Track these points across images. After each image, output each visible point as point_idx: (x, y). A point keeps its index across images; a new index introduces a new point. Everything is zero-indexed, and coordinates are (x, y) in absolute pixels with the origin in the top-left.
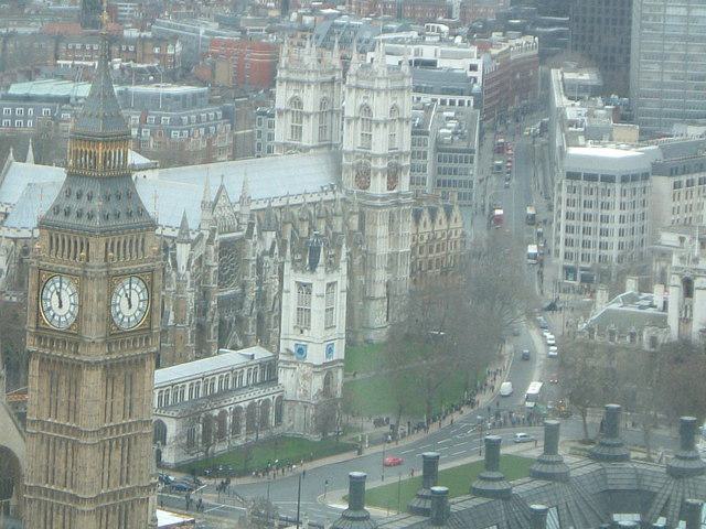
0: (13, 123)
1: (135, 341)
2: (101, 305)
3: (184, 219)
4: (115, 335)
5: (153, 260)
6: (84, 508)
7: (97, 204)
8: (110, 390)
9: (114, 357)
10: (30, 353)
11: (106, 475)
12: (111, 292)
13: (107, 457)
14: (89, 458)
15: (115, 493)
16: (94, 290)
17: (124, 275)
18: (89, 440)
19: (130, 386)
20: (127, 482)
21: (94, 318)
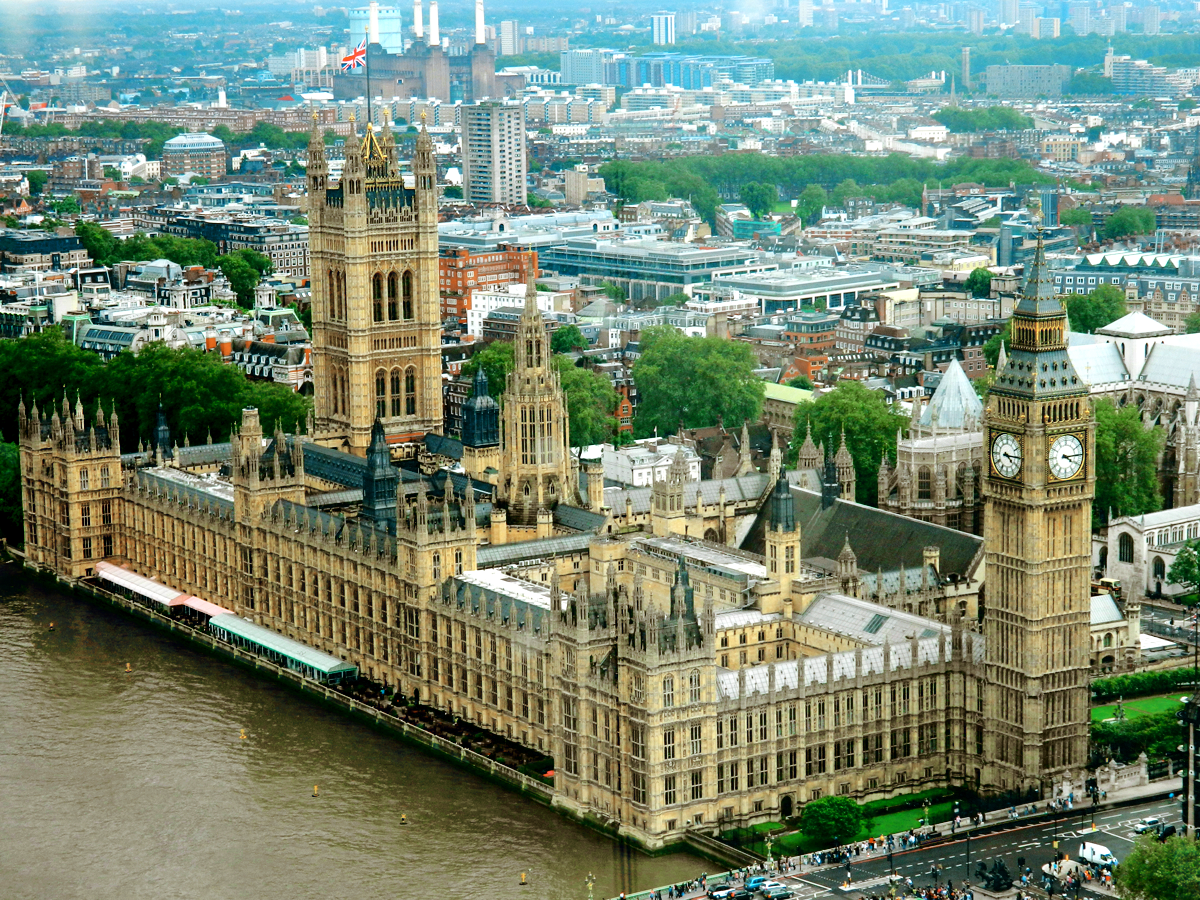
0: (1075, 290)
2: (1040, 458)
3: (1192, 380)
4: (1052, 485)
6: (1035, 629)
9: (1053, 501)
10: (985, 498)
11: (1051, 602)
12: (1048, 447)
13: (1051, 587)
14: (1037, 589)
15: (1059, 617)
17: (1059, 433)
19: (1069, 528)
21: (1034, 468)
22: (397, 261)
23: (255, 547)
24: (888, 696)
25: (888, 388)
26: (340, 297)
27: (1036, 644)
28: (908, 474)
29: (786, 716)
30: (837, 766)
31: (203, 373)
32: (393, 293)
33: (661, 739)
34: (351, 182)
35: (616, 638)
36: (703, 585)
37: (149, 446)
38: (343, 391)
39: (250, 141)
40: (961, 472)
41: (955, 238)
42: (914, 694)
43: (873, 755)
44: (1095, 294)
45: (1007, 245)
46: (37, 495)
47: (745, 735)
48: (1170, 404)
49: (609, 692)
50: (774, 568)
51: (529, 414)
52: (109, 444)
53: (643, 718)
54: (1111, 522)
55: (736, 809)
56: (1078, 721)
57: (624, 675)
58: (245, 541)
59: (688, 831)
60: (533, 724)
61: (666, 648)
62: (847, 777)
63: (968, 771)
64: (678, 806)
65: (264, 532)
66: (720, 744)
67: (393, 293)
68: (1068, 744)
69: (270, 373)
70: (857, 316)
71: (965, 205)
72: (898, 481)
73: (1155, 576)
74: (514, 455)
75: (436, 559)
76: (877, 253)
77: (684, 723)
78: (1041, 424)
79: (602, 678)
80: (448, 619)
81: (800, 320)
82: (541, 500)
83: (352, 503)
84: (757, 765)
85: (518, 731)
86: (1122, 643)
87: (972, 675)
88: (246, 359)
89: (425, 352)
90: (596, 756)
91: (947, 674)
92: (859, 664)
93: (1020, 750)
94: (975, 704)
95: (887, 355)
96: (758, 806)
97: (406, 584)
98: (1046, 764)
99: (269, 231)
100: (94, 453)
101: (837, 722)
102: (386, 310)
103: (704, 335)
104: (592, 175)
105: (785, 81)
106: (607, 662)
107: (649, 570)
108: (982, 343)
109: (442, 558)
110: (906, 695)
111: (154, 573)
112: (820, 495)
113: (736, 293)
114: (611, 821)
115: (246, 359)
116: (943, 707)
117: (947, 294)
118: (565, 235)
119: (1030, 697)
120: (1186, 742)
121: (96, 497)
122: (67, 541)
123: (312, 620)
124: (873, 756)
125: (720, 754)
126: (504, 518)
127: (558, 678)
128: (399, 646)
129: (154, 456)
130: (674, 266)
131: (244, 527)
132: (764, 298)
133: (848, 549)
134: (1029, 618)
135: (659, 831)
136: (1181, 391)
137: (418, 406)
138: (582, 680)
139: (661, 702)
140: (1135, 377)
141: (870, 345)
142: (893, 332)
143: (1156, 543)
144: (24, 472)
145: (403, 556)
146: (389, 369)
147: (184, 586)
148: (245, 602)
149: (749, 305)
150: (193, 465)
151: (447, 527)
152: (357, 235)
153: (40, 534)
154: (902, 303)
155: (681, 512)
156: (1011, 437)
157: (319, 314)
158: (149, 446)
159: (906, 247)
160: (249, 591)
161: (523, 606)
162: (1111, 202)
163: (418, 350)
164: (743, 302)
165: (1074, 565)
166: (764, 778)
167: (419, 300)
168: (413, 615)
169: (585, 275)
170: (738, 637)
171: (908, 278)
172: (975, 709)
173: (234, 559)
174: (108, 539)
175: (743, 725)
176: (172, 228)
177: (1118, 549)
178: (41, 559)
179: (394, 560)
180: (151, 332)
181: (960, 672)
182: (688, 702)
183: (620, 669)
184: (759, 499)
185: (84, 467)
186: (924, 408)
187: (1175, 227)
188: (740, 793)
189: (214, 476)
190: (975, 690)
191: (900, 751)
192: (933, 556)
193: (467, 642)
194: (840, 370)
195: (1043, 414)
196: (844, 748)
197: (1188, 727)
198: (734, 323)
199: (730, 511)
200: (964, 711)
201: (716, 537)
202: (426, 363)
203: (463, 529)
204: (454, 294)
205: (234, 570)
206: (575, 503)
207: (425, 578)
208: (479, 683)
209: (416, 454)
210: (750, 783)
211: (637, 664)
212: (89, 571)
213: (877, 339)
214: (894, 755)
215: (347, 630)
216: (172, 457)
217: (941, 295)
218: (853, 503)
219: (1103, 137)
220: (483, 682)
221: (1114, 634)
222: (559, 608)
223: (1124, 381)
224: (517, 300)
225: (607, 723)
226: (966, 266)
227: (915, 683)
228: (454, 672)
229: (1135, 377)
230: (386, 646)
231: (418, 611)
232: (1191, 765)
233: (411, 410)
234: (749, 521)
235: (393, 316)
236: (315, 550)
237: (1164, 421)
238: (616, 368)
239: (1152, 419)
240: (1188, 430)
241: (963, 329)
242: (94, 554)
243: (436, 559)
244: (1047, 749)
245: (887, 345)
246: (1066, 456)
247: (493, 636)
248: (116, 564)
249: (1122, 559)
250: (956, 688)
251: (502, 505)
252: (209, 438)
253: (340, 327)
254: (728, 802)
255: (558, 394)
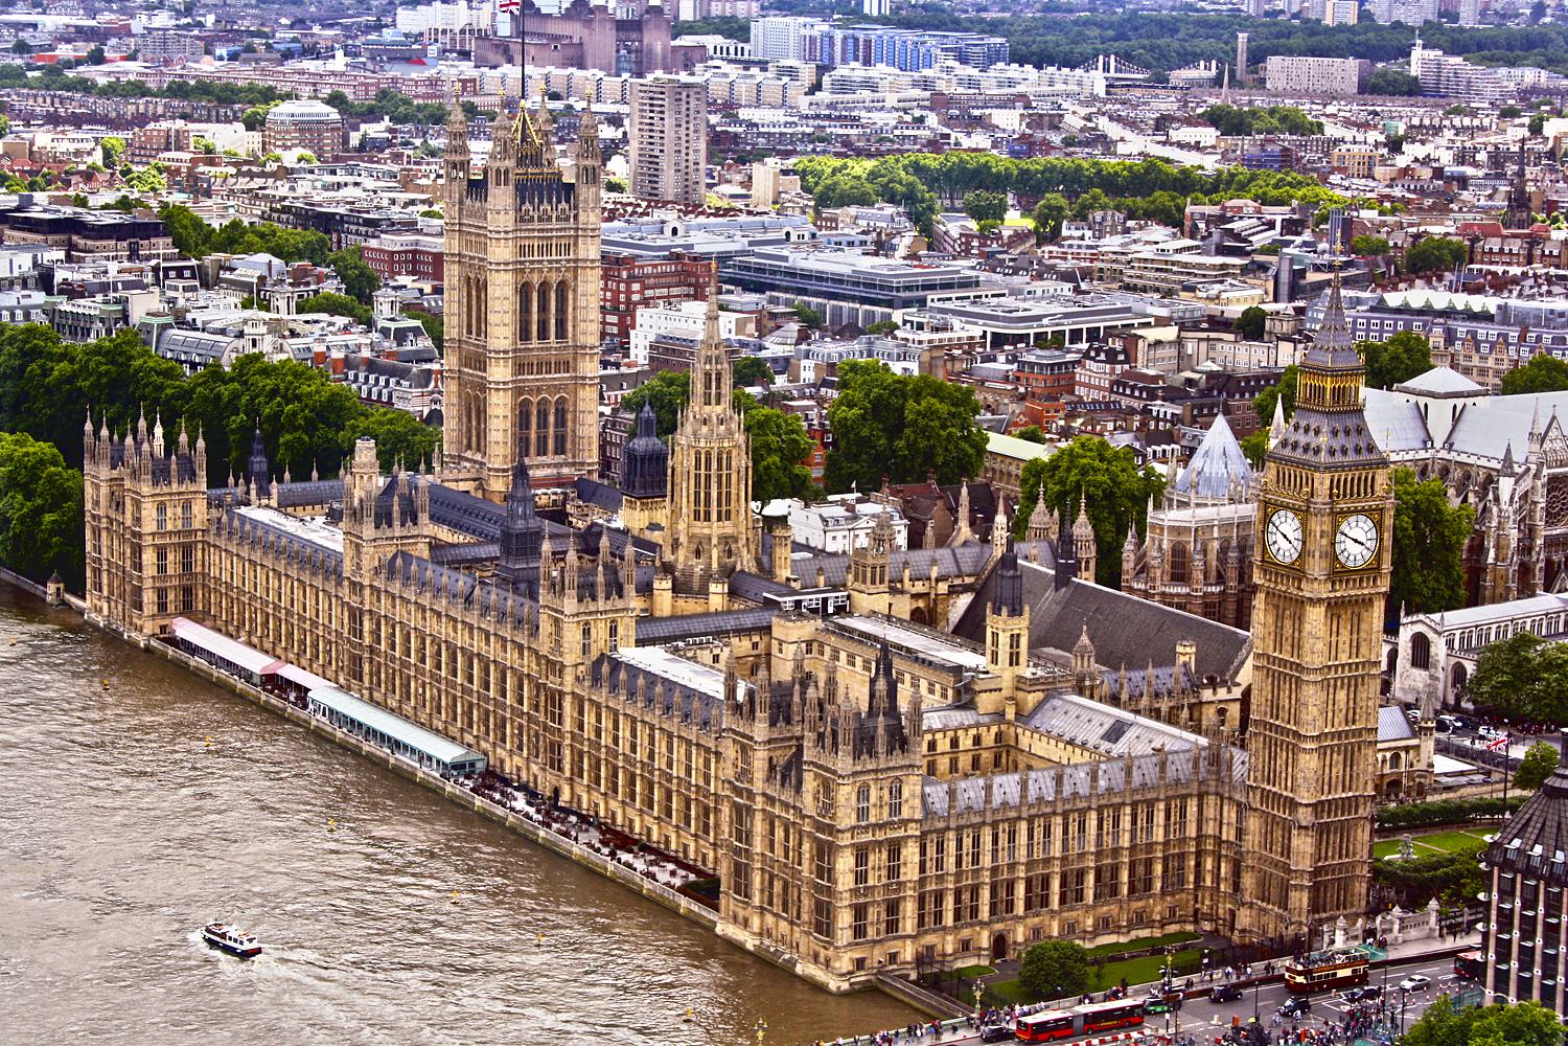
0: (1367, 336)
1: (1361, 580)
2: (1324, 542)
3: (1508, 451)
4: (1338, 573)
5: (1382, 498)
7: (1323, 440)
8: (1335, 628)
10: (1256, 586)
11: (1330, 714)
12: (1335, 528)
14: (1312, 696)
15: (1340, 733)
16: (1318, 525)
17: (1350, 512)
18: (1312, 677)
19: (1356, 628)
20: (1354, 723)
21: (1317, 554)
22: (550, 269)
23: (367, 607)
24: (1128, 818)
25: (1137, 445)
26: (479, 309)
27: (1309, 763)
28: (1158, 546)
29: (1003, 839)
30: (1063, 901)
31: (310, 395)
32: (543, 308)
33: (852, 861)
34: (498, 171)
35: (802, 737)
36: (907, 677)
37: (241, 481)
38: (479, 423)
39: (372, 115)
40: (1224, 550)
41: (1223, 266)
42: (1159, 818)
43: (1107, 886)
44: (1392, 342)
45: (1285, 277)
46: (104, 534)
47: (952, 860)
48: (1481, 478)
49: (791, 801)
50: (995, 660)
51: (703, 459)
52: (193, 477)
53: (830, 835)
54: (1404, 620)
55: (940, 947)
56: (1358, 858)
57: (810, 783)
58: (354, 602)
59: (879, 972)
60: (696, 835)
61: (861, 753)
62: (1074, 914)
63: (1221, 911)
64: (868, 942)
65: (379, 591)
66: (922, 869)
67: (543, 308)
68: (1345, 885)
69: (390, 397)
70: (1102, 357)
71: (1236, 226)
72: (1147, 559)
73: (1454, 686)
74: (684, 510)
75: (586, 632)
76: (1127, 280)
77: (880, 843)
78: (1327, 500)
79: (783, 785)
80: (598, 706)
81: (1032, 359)
82: (715, 566)
83: (486, 559)
84: (966, 897)
85: (678, 843)
86: (1412, 765)
87: (1230, 798)
88: (361, 379)
89: (581, 381)
90: (772, 877)
91: (1201, 797)
92: (1094, 778)
93: (1285, 889)
94: (1233, 832)
95: (1136, 404)
96: (965, 946)
97: (548, 661)
98: (1315, 907)
99: (393, 224)
100: (175, 487)
101: (1065, 847)
102: (535, 328)
103: (916, 373)
104: (785, 172)
105: (1021, 65)
106: (788, 767)
107: (843, 656)
108: (1252, 395)
109: (593, 631)
110: (1150, 818)
111: (242, 633)
112: (1053, 572)
113: (956, 322)
114: (787, 956)
115: (361, 379)
116: (1194, 835)
117: (1213, 335)
118: (751, 243)
119: (1300, 827)
120: (1489, 891)
121: (175, 540)
122: (138, 591)
123: (432, 698)
124: (1107, 890)
125: (922, 882)
126: (670, 585)
127: (730, 782)
128: (537, 735)
129: (248, 492)
130: (882, 287)
131: (353, 584)
132: (989, 330)
133: (1085, 639)
134: (1302, 732)
135: (844, 971)
136: (1494, 464)
137: (569, 446)
138: (758, 786)
139: (854, 816)
140: (1438, 444)
141: (1117, 393)
142: (1144, 377)
143: (1456, 646)
144: (88, 506)
145: (546, 627)
146: (535, 400)
147: (279, 651)
148: (352, 674)
149: (972, 338)
150: (294, 505)
151: (601, 595)
152: (502, 235)
153: (105, 581)
154: (1158, 343)
155: (884, 587)
156: (1290, 515)
157: (452, 329)
158: (241, 481)
159: (1163, 275)
160: (356, 661)
161: (689, 694)
162: (1414, 230)
163: (572, 378)
164: (964, 334)
165: (1360, 672)
166: (974, 911)
167: (574, 318)
168: (555, 699)
169: (775, 294)
170: (948, 741)
171: (1164, 312)
172: (1232, 838)
173: (339, 620)
174: (188, 591)
175: (951, 846)
176: (275, 215)
177: (1410, 651)
178: (105, 611)
179: (535, 631)
180: (245, 343)
181: (1217, 794)
182: (885, 817)
183: (805, 774)
184: (977, 575)
185: (162, 503)
186: (1181, 472)
187: (1491, 263)
188: (945, 928)
189: (320, 520)
190: (1234, 820)
191: (1140, 886)
192: (1186, 653)
193: (621, 734)
194: (1080, 421)
195: (1331, 489)
196: (1072, 879)
197: (1491, 872)
198: (953, 358)
199: (943, 588)
200: (1218, 840)
201: (924, 618)
202: (582, 393)
203: (621, 597)
204: (615, 310)
205: (339, 634)
206: (754, 570)
207: (571, 656)
208: (633, 783)
209: (564, 504)
210: (957, 916)
211: (827, 770)
212: (163, 628)
213: (1125, 386)
214: (1132, 890)
215: (475, 712)
216: (269, 495)
217: (1204, 335)
218: (1092, 584)
219: (1405, 147)
220: (638, 783)
221: (1403, 755)
222: (735, 698)
223: (1426, 450)
224: (691, 321)
225: (787, 839)
226: (1238, 300)
227: (1162, 806)
228: (603, 769)
229: (1438, 444)
230: (521, 734)
231: (562, 694)
232: (1494, 917)
233: (560, 449)
234: (965, 600)
235: (543, 334)
236: (439, 615)
237: (1472, 499)
238: (810, 408)
239: (1458, 496)
240: (1500, 511)
241: (1230, 377)
242: (171, 608)
243: (586, 632)
244: (1318, 890)
245: (1137, 394)
246: (1358, 540)
247: (652, 728)
248: (200, 622)
249: (1414, 664)
250: (1210, 812)
251: (668, 569)
252: (315, 474)
253: (477, 346)
254: (930, 939)
255: (740, 438)
